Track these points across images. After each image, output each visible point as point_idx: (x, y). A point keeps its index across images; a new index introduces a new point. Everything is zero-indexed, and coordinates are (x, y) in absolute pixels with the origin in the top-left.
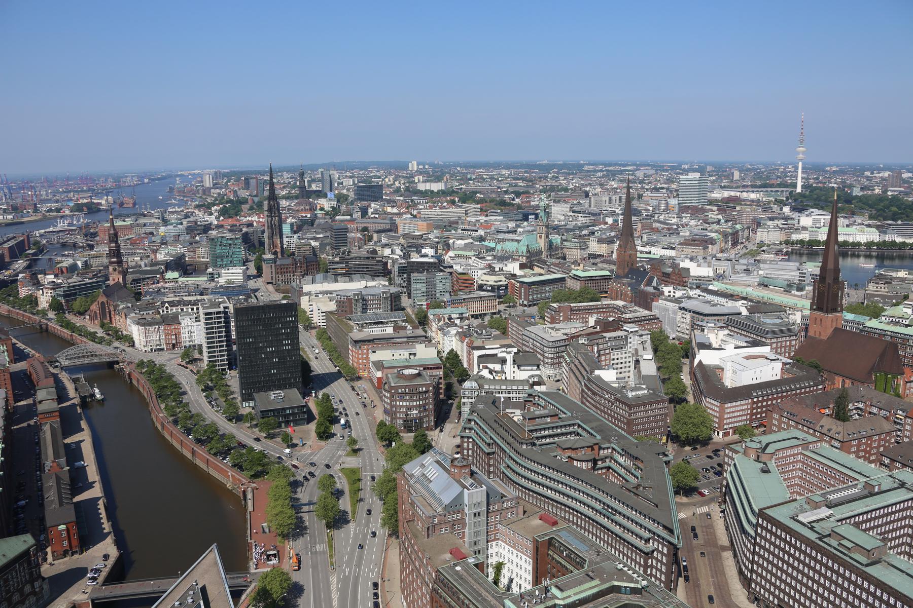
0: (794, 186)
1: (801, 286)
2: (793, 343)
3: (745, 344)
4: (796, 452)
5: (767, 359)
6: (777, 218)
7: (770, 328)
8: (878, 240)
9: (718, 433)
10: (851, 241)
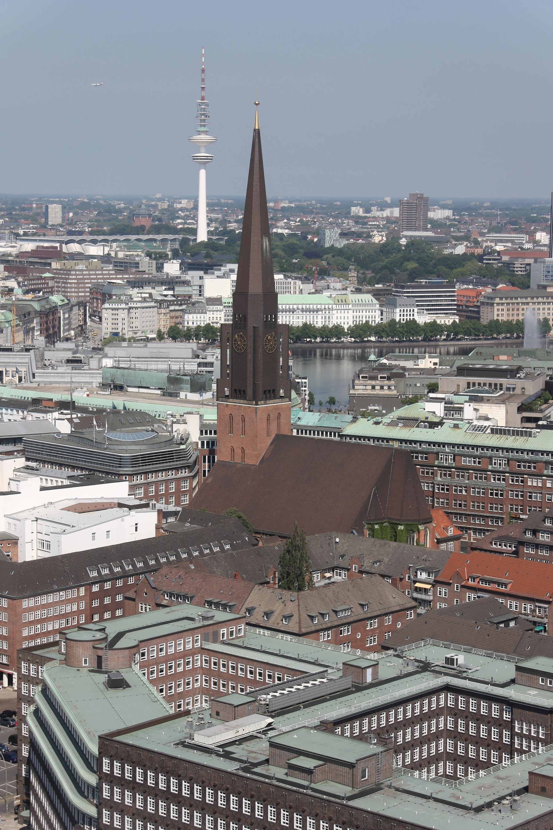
0: (194, 232)
1: (202, 380)
2: (185, 487)
3: (66, 482)
4: (189, 646)
5: (121, 505)
6: (149, 282)
7: (127, 451)
8: (378, 320)
9: (10, 677)
10: (319, 325)
